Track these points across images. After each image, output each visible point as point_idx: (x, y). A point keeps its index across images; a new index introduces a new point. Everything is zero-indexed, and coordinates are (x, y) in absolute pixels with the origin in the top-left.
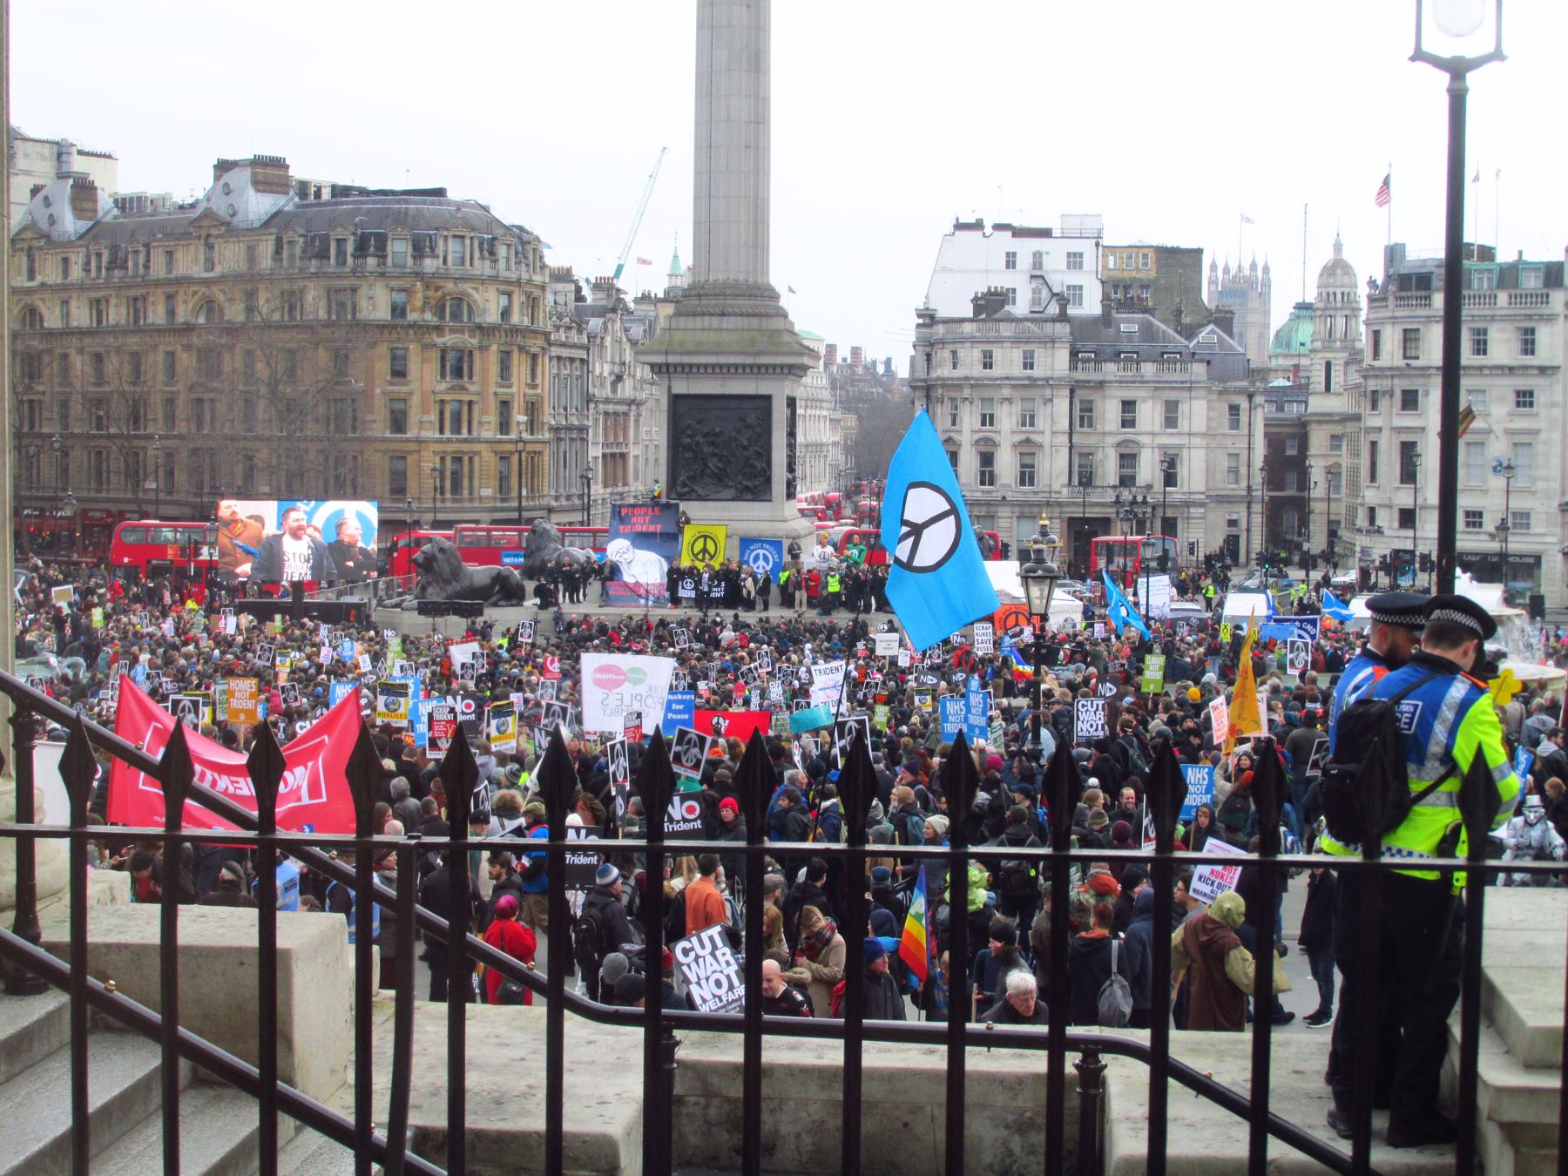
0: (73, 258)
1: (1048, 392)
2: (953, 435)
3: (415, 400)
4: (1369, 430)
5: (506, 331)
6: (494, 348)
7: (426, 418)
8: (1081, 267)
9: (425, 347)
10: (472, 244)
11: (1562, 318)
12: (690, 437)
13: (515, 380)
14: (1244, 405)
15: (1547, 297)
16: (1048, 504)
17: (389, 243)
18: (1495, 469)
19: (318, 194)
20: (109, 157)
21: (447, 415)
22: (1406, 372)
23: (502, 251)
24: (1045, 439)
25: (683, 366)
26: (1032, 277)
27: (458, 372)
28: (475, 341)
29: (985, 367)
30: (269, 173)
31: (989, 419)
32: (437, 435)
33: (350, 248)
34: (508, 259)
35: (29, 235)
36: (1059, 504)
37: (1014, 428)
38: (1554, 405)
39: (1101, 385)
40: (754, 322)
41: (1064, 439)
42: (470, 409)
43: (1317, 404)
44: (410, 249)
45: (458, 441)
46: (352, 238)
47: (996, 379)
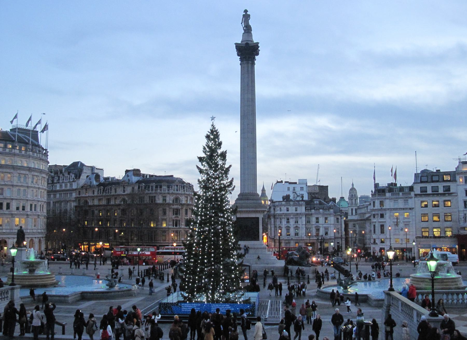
0: (95, 190)
1: (301, 216)
4: (373, 222)
6: (184, 208)
9: (170, 208)
13: (188, 215)
14: (340, 218)
16: (301, 240)
19: (146, 177)
20: (102, 170)
23: (185, 188)
24: (300, 226)
26: (293, 192)
27: (176, 214)
28: (180, 207)
30: (136, 172)
31: (288, 222)
32: (172, 227)
36: (304, 240)
38: (413, 216)
39: (312, 214)
40: (255, 201)
41: (304, 226)
42: (179, 222)
43: (349, 218)
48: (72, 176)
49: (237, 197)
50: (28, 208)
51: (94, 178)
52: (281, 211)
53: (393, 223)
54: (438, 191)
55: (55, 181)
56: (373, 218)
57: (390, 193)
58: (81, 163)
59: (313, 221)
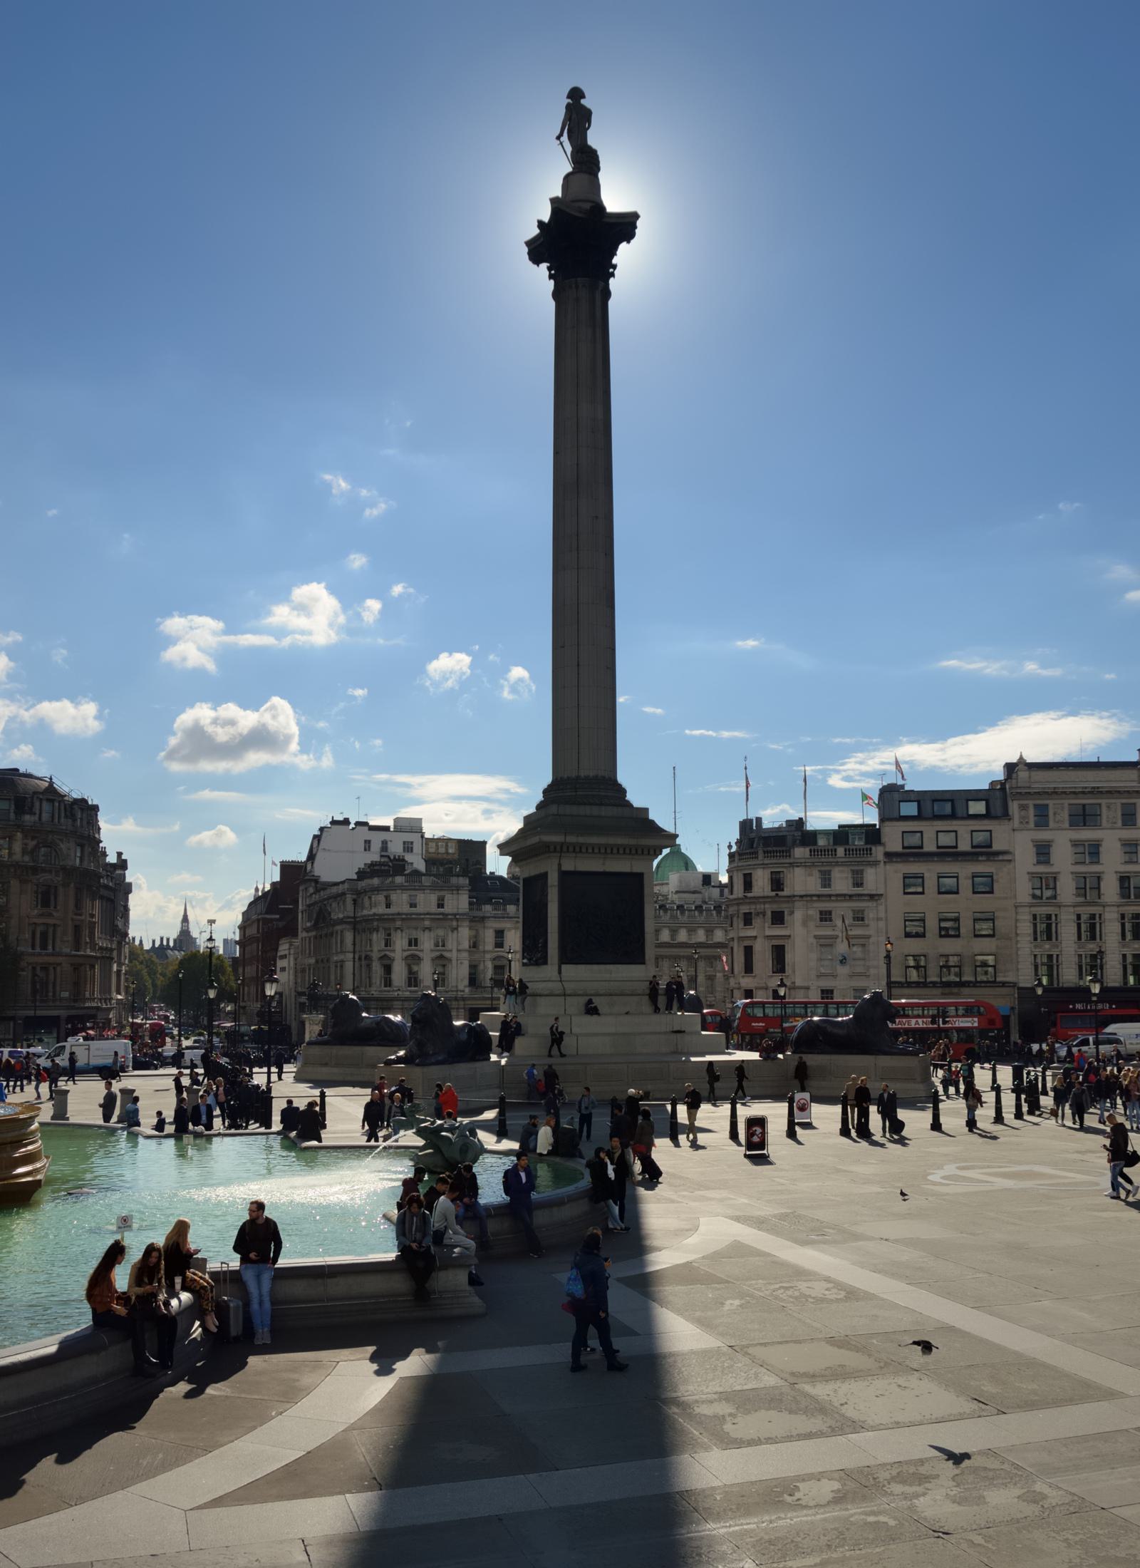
1: (455, 923)
2: (388, 953)
4: (741, 939)
6: (72, 885)
8: (412, 851)
11: (882, 863)
15: (871, 850)
18: (841, 962)
21: (38, 935)
22: (777, 899)
24: (454, 955)
29: (411, 907)
31: (413, 942)
32: (30, 950)
34: (81, 819)
36: (464, 999)
37: (432, 947)
38: (878, 919)
41: (465, 955)
44: (13, 807)
45: (48, 955)
47: (421, 914)
49: (540, 797)
52: (388, 906)
53: (814, 941)
54: (956, 847)
56: (741, 925)
57: (807, 850)
59: (486, 940)
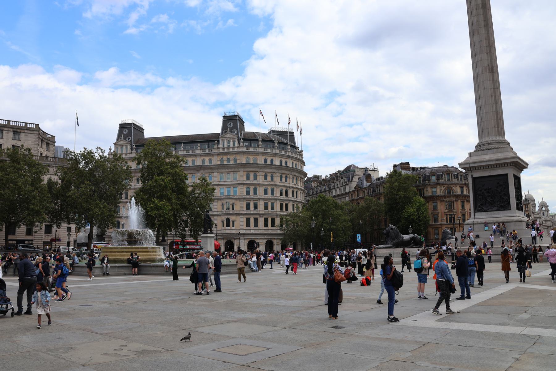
3: (440, 215)
5: (462, 196)
6: (460, 201)
7: (443, 219)
10: (452, 175)
12: (481, 191)
13: (466, 208)
17: (431, 177)
23: (459, 177)
25: (475, 167)
30: (405, 166)
33: (421, 179)
34: (461, 179)
35: (357, 187)
42: (454, 218)
44: (436, 178)
46: (422, 177)
48: (344, 180)
50: (277, 208)
51: (365, 179)
55: (332, 188)
58: (354, 166)
